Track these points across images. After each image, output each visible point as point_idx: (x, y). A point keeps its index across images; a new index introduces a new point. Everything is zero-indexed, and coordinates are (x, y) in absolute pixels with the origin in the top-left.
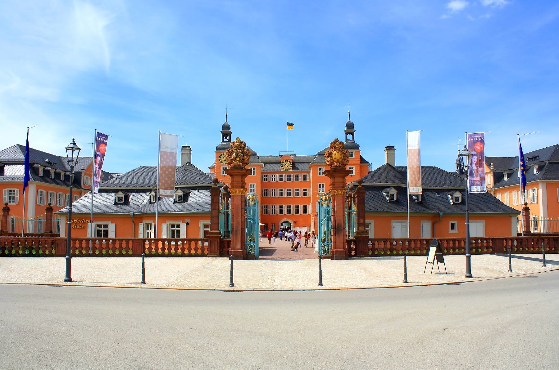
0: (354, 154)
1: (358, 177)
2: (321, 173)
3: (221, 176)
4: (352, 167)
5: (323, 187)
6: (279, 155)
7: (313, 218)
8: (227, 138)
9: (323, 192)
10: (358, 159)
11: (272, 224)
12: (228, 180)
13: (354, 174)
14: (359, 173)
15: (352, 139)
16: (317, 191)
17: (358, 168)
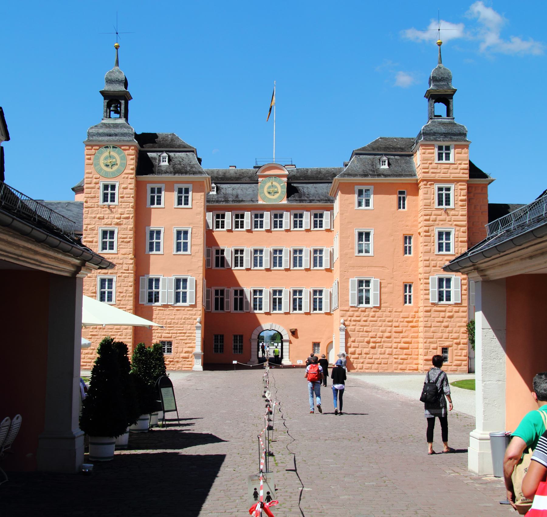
0: (452, 152)
1: (461, 213)
2: (364, 203)
3: (98, 206)
4: (447, 185)
5: (367, 239)
6: (255, 167)
7: (342, 321)
8: (119, 109)
9: (367, 251)
10: (463, 166)
11: (235, 336)
12: (118, 218)
13: (452, 206)
14: (465, 203)
15: (444, 115)
16: (353, 248)
17: (461, 189)
